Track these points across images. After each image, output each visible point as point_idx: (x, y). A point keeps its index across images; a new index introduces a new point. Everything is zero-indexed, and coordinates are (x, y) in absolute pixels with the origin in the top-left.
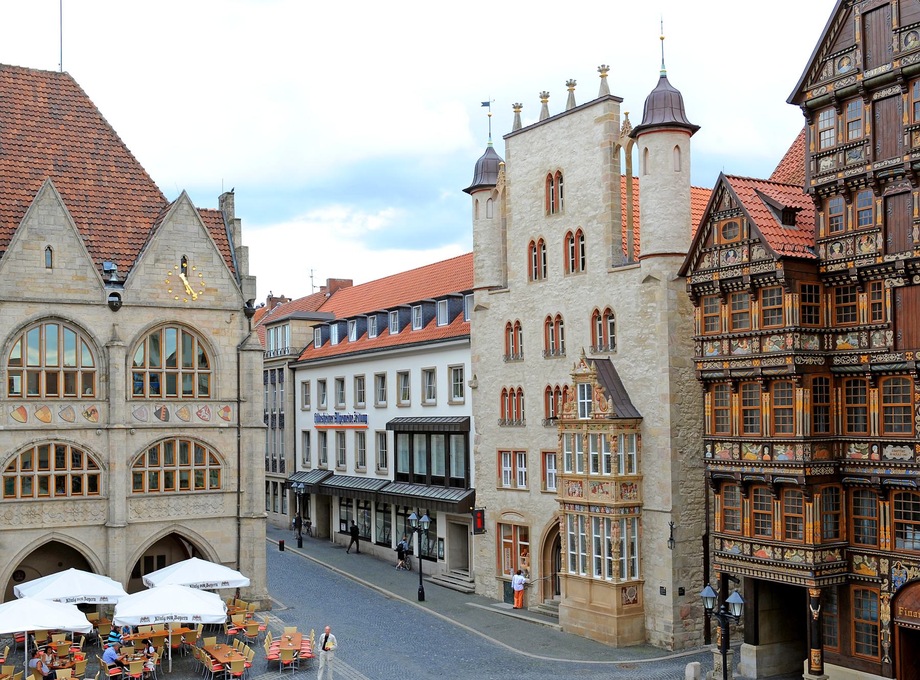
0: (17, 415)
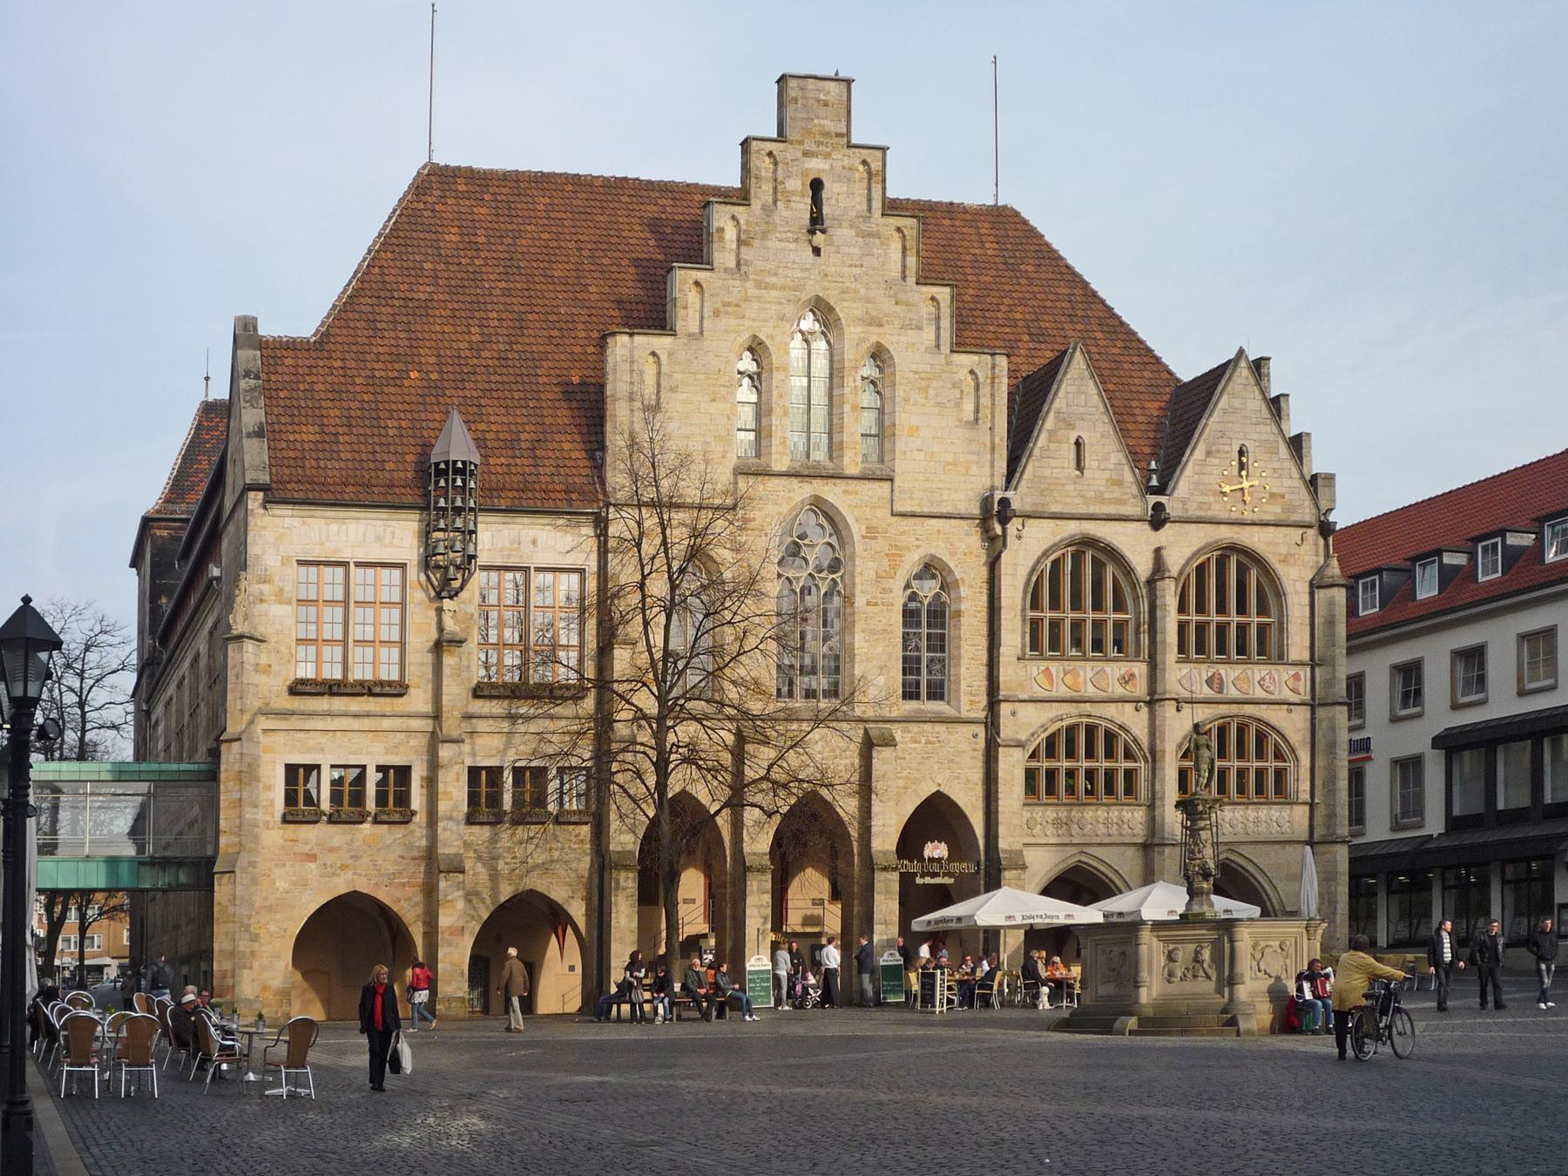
0: (1042, 680)
